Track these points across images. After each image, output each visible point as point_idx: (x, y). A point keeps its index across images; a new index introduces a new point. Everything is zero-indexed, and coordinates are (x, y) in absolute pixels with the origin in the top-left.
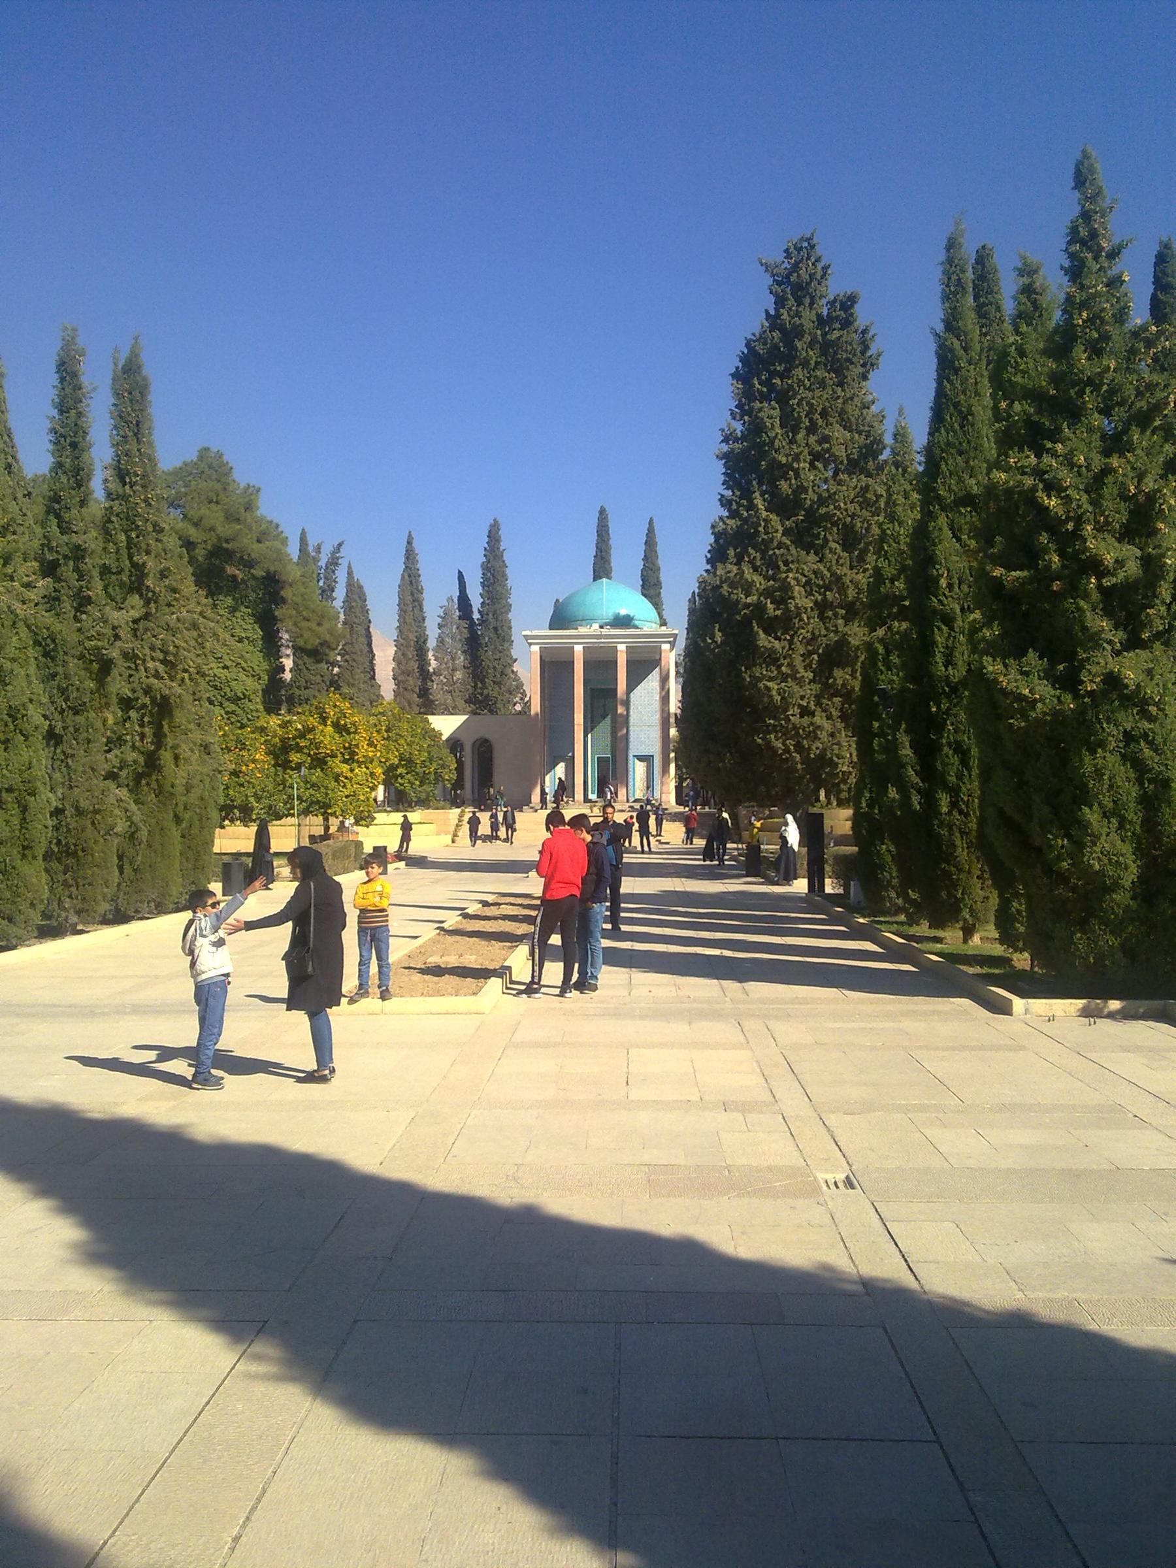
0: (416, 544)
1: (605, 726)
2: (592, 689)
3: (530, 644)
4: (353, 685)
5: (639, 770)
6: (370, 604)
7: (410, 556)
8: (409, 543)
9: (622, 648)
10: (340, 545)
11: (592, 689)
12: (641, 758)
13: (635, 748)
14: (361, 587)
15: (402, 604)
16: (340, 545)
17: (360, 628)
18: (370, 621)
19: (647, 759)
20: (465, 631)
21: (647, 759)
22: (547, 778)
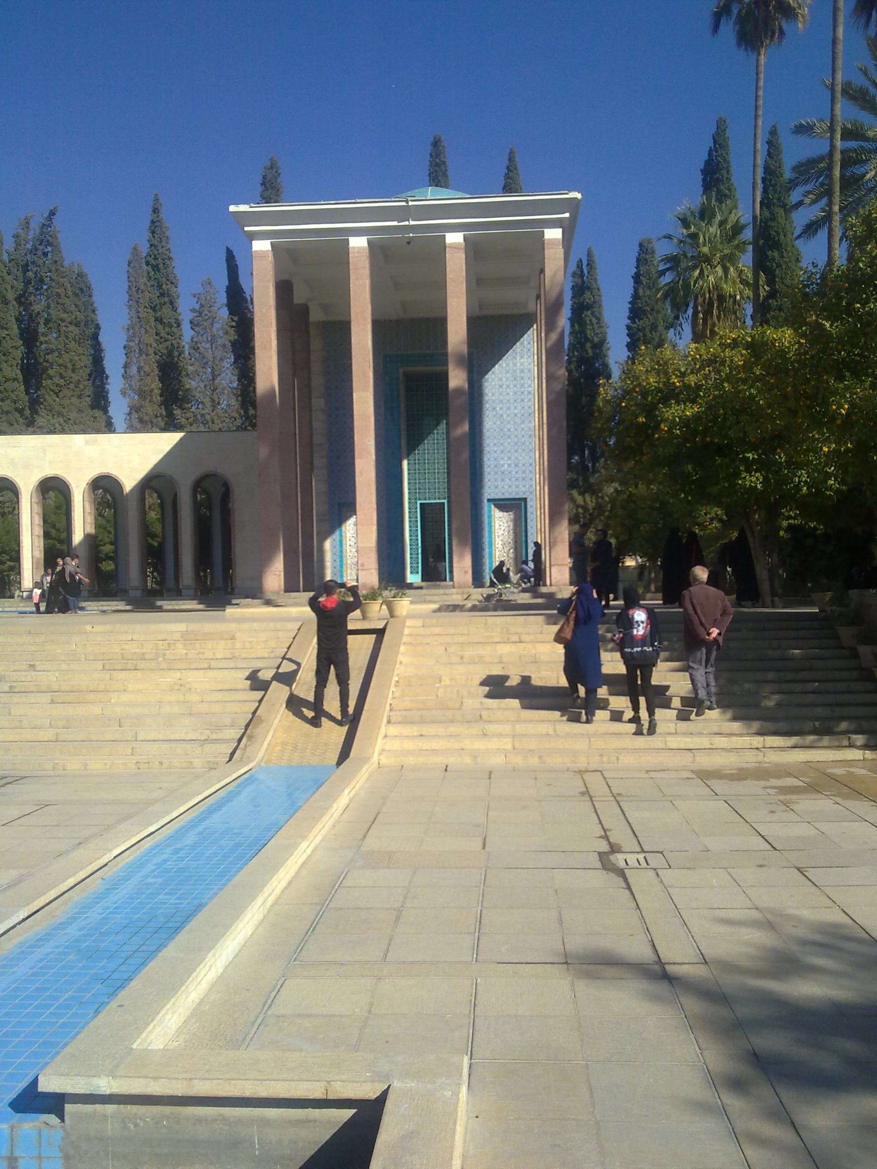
0: (163, 215)
1: (434, 447)
3: (253, 236)
5: (499, 527)
6: (98, 299)
7: (155, 227)
8: (155, 211)
9: (454, 238)
12: (503, 505)
14: (81, 275)
15: (134, 291)
18: (98, 327)
19: (515, 506)
20: (232, 331)
21: (515, 506)
22: (328, 545)
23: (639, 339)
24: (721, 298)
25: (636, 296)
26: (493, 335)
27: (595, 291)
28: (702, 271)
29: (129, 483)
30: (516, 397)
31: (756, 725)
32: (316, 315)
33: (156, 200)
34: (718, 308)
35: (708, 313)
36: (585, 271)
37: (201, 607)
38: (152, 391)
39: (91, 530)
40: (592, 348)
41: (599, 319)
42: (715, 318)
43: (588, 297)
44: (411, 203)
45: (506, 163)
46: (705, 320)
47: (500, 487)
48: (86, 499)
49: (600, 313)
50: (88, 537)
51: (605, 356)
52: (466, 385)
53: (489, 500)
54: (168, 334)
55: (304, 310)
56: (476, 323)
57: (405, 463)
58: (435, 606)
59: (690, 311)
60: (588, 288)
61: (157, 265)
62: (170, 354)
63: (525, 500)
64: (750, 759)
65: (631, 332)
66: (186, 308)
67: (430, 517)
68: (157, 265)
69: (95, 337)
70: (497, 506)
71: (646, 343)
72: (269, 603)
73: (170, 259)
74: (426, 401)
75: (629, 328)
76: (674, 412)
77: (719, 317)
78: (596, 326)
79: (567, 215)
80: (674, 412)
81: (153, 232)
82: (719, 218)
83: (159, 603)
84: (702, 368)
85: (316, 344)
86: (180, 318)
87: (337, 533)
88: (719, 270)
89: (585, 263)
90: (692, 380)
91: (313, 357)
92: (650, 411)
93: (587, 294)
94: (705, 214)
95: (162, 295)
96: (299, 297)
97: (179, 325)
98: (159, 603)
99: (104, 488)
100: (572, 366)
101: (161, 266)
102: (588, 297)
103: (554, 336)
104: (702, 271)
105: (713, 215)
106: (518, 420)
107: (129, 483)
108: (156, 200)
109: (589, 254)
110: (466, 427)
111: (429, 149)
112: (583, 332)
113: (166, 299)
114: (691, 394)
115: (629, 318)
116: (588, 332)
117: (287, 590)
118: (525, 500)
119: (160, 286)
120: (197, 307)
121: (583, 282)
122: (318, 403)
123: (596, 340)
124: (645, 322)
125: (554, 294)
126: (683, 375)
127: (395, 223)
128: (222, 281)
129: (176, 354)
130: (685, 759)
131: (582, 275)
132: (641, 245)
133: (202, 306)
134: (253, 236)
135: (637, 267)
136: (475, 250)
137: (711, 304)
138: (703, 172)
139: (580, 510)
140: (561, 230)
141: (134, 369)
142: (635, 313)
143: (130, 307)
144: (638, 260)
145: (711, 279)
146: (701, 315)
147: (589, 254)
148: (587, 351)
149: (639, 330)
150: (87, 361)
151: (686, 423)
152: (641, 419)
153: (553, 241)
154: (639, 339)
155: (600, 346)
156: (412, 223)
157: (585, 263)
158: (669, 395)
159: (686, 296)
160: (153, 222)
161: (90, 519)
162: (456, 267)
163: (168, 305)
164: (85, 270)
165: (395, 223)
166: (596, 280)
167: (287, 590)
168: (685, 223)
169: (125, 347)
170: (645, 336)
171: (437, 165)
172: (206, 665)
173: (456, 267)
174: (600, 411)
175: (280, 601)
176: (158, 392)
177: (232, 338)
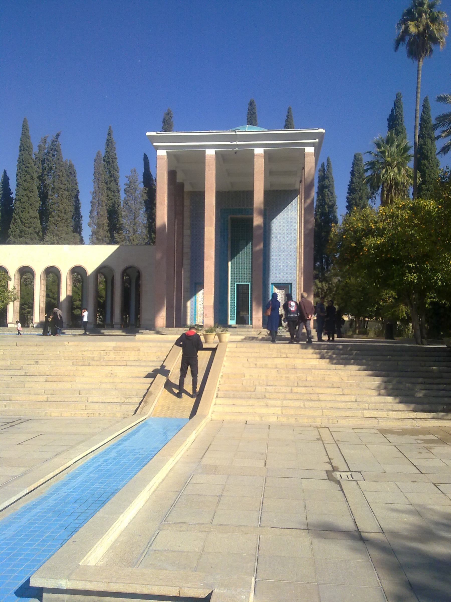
1: (245, 256)
2: (234, 221)
3: (157, 148)
4: (57, 235)
6: (79, 179)
7: (109, 143)
8: (109, 134)
9: (259, 151)
10: (58, 135)
11: (234, 221)
12: (279, 286)
13: (275, 276)
14: (71, 166)
15: (97, 174)
16: (58, 135)
17: (65, 192)
18: (78, 192)
20: (145, 195)
22: (189, 304)
23: (353, 204)
24: (397, 184)
25: (352, 182)
26: (277, 200)
27: (331, 179)
28: (387, 170)
29: (90, 269)
30: (288, 232)
31: (412, 406)
32: (187, 188)
33: (110, 129)
34: (395, 189)
35: (389, 191)
36: (326, 169)
37: (124, 334)
38: (103, 224)
39: (70, 293)
40: (328, 208)
41: (332, 194)
42: (393, 194)
43: (326, 182)
44: (237, 133)
45: (286, 114)
46: (388, 195)
47: (278, 277)
48: (68, 277)
49: (333, 190)
50: (68, 297)
51: (335, 212)
52: (263, 225)
53: (272, 284)
54: (113, 196)
55: (182, 186)
56: (269, 194)
57: (230, 263)
58: (243, 337)
59: (380, 190)
60: (327, 178)
61: (109, 162)
62: (114, 205)
63: (291, 284)
64: (408, 424)
65: (349, 200)
66: (122, 183)
67: (242, 292)
68: (109, 162)
69: (76, 197)
70: (276, 287)
71: (357, 205)
72: (158, 333)
73: (115, 158)
74: (242, 231)
75: (347, 198)
76: (371, 241)
77: (395, 194)
78: (330, 197)
79: (317, 140)
80: (371, 241)
81: (108, 145)
82: (396, 143)
83: (102, 331)
84: (386, 219)
85: (187, 202)
86: (119, 188)
87: (194, 298)
88: (396, 170)
89: (326, 165)
90: (381, 225)
91: (185, 209)
92: (358, 241)
93: (326, 181)
94: (389, 141)
95: (111, 176)
96: (180, 178)
97: (118, 192)
98: (102, 331)
99: (78, 272)
100: (318, 217)
101: (111, 162)
102: (326, 182)
103: (309, 201)
104: (387, 170)
105: (393, 142)
106: (289, 243)
107: (90, 269)
108: (110, 129)
109: (328, 160)
110: (261, 246)
111: (248, 106)
112: (323, 199)
113: (113, 179)
114: (380, 233)
115: (348, 193)
116: (326, 200)
117: (168, 326)
118: (291, 284)
119: (110, 172)
120: (128, 182)
121: (324, 174)
122: (187, 232)
123: (330, 204)
124: (356, 195)
125: (309, 180)
126: (376, 222)
127: (229, 143)
128: (141, 171)
129: (116, 206)
130: (374, 423)
131: (324, 171)
132: (355, 156)
133: (130, 182)
134: (157, 148)
135: (353, 167)
136: (269, 157)
137: (391, 187)
138: (389, 120)
139: (320, 290)
140: (314, 148)
141: (95, 213)
142: (351, 191)
143: (94, 182)
144: (353, 164)
145: (392, 174)
146: (386, 192)
147: (328, 160)
148: (325, 209)
149: (353, 199)
150: (72, 209)
151: (377, 247)
152: (353, 245)
153: (309, 154)
154: (353, 204)
155: (332, 207)
156: (238, 143)
157: (326, 165)
158: (368, 232)
159: (378, 182)
160: (108, 140)
161: (70, 288)
162: (259, 165)
163: (114, 182)
164: (73, 163)
165: (229, 143)
166: (331, 174)
167: (168, 326)
168: (379, 146)
169: (91, 202)
170: (356, 202)
171: (252, 114)
172: (125, 364)
173: (259, 165)
174: (332, 240)
175: (163, 332)
176: (107, 225)
177: (145, 199)
